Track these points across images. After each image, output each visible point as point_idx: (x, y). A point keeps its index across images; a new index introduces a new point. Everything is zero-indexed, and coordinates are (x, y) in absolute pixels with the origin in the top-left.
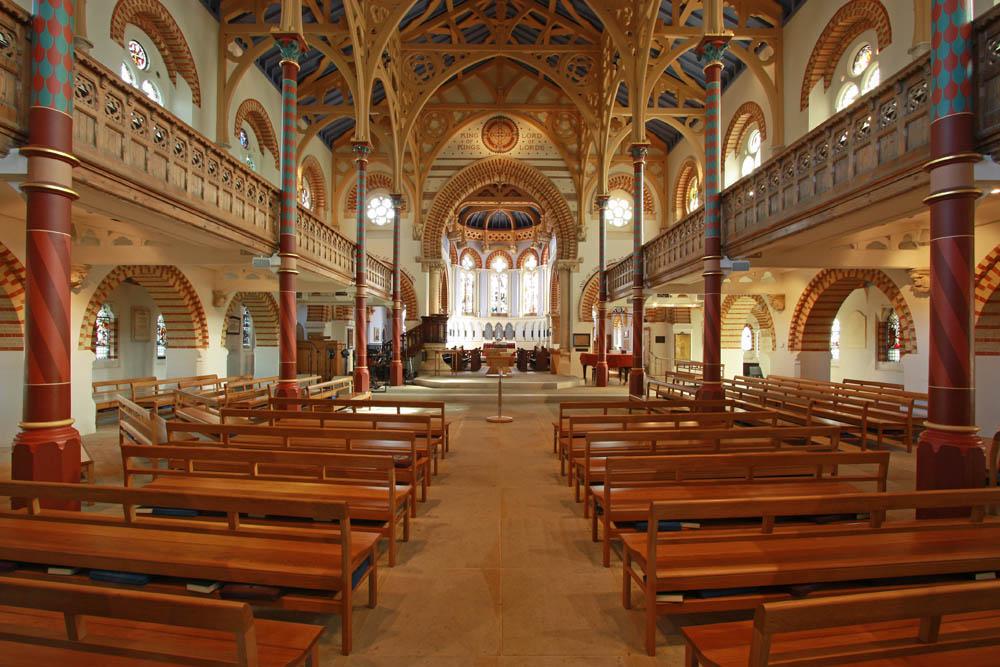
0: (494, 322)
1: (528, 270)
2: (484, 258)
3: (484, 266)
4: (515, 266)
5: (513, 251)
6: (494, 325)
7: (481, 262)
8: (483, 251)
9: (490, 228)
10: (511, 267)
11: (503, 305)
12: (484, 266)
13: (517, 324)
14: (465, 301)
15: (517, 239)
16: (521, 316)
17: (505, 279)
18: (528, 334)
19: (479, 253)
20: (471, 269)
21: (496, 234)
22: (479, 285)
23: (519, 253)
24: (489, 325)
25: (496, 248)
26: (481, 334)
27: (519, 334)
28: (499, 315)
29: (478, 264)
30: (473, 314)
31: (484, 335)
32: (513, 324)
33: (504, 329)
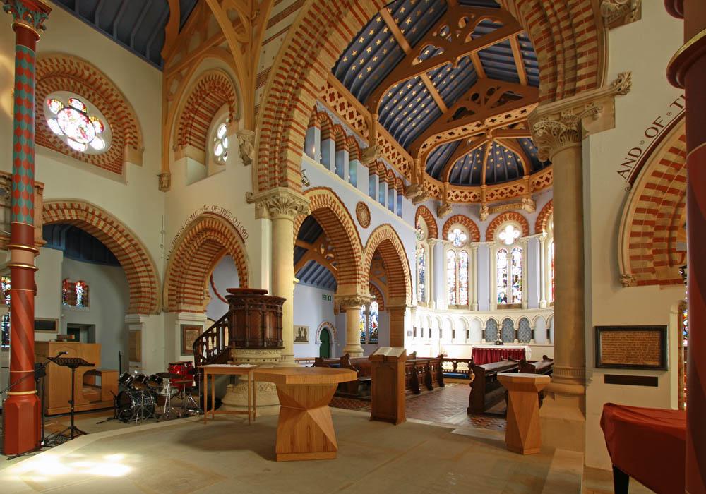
0: (500, 317)
3: (483, 237)
4: (532, 230)
5: (527, 208)
7: (478, 233)
8: (480, 217)
9: (490, 181)
10: (526, 233)
11: (516, 293)
12: (483, 237)
13: (537, 318)
15: (536, 189)
17: (517, 256)
19: (476, 220)
20: (464, 244)
21: (501, 188)
23: (539, 210)
24: (491, 321)
25: (500, 210)
26: (480, 334)
28: (509, 307)
30: (468, 306)
31: (484, 337)
32: (530, 320)
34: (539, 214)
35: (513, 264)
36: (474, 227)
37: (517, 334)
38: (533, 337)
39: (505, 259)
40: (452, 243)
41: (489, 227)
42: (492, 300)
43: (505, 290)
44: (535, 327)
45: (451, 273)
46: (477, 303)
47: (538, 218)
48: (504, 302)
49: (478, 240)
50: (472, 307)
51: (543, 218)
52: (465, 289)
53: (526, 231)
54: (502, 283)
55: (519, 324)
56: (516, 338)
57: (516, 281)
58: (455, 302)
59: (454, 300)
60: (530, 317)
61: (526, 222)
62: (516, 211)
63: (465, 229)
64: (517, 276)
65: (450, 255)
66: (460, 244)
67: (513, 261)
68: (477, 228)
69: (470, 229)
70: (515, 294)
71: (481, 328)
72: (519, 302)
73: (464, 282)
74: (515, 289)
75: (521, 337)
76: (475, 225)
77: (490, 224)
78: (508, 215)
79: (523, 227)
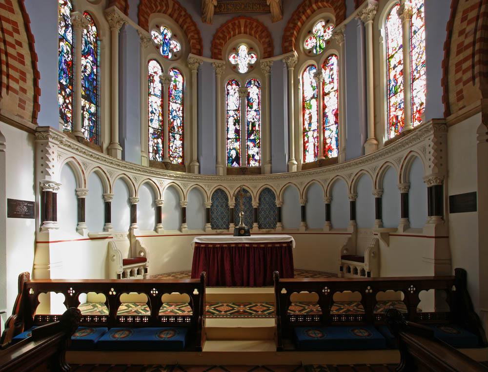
0: (231, 187)
1: (309, 53)
2: (207, 32)
3: (207, 50)
4: (277, 48)
6: (231, 192)
7: (200, 41)
10: (268, 53)
11: (253, 151)
12: (207, 50)
13: (285, 189)
14: (160, 134)
16: (294, 169)
17: (254, 92)
18: (316, 212)
19: (197, 19)
22: (202, 102)
24: (220, 194)
27: (291, 214)
28: (244, 171)
29: (193, 43)
30: (181, 167)
31: (208, 219)
32: (277, 191)
33: (255, 204)
34: (289, 22)
35: (248, 106)
36: (193, 28)
37: (255, 216)
38: (280, 220)
39: (237, 95)
40: (157, 47)
41: (215, 37)
42: (220, 160)
43: (237, 145)
44: (283, 202)
45: (155, 102)
46: (198, 161)
47: (287, 29)
48: (235, 165)
49: (200, 53)
50: (189, 166)
51: (294, 28)
52: (177, 137)
53: (269, 49)
54: (231, 135)
55: (260, 199)
56: (256, 222)
57: (252, 131)
58: (163, 156)
59: (161, 152)
60: (276, 187)
61: (269, 35)
62: (254, 17)
63: (180, 33)
64: (253, 125)
65: (154, 67)
66: (170, 56)
67: (249, 100)
68: (198, 33)
69: (186, 33)
70: (251, 152)
71: (203, 204)
72: (257, 164)
73: (178, 122)
74: (251, 144)
75: (262, 221)
76: (194, 24)
77: (217, 31)
78: (242, 22)
79: (264, 43)
